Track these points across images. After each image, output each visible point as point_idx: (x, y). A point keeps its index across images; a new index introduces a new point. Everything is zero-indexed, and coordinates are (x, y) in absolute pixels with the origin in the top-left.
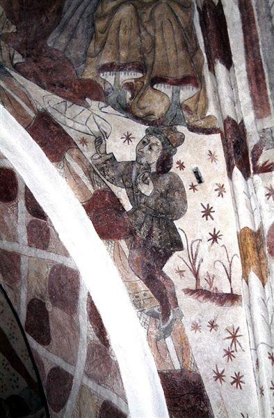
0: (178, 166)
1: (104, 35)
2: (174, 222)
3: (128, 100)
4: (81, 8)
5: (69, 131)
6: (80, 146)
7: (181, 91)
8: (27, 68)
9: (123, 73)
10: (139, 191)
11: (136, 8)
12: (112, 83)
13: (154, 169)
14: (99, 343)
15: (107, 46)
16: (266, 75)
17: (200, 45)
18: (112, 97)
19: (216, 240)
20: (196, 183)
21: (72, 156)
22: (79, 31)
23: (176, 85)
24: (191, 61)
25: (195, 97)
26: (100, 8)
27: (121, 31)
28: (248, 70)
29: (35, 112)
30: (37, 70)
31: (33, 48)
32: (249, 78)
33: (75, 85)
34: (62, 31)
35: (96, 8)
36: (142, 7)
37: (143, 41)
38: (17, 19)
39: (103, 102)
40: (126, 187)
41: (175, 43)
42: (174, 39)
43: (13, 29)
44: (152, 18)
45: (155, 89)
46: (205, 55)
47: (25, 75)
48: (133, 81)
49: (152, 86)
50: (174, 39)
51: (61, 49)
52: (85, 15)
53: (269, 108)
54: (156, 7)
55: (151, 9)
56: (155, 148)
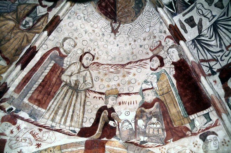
11: (15, 26)
16: (29, 82)
24: (14, 56)
27: (4, 26)
28: (26, 76)
32: (24, 78)
35: (5, 13)
36: (17, 28)
37: (7, 36)
46: (19, 59)
53: (20, 92)
54: (21, 32)
55: (19, 31)
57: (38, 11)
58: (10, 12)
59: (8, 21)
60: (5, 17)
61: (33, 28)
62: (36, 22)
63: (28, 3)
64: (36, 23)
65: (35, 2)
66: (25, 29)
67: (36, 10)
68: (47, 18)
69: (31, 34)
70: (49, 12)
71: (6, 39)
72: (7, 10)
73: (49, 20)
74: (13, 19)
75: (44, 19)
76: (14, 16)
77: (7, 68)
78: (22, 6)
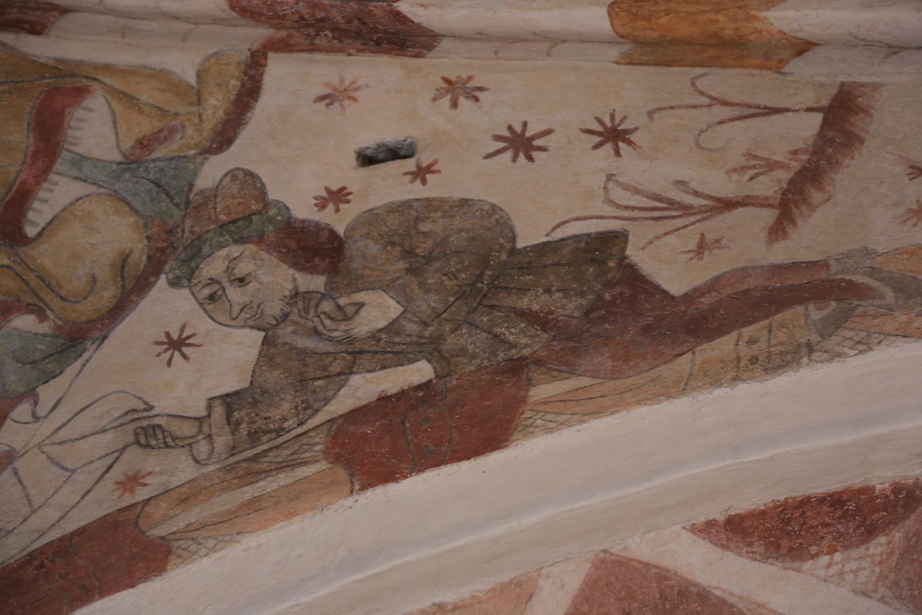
0: (331, 207)
2: (520, 244)
3: (45, 328)
5: (70, 526)
6: (141, 494)
7: (81, 150)
10: (374, 336)
13: (316, 282)
14: (897, 535)
19: (626, 132)
20: (410, 164)
21: (167, 518)
23: (52, 162)
25: (116, 105)
39: (12, 408)
40: (349, 371)
45: (40, 234)
49: (25, 241)
56: (243, 268)
77: (109, 81)
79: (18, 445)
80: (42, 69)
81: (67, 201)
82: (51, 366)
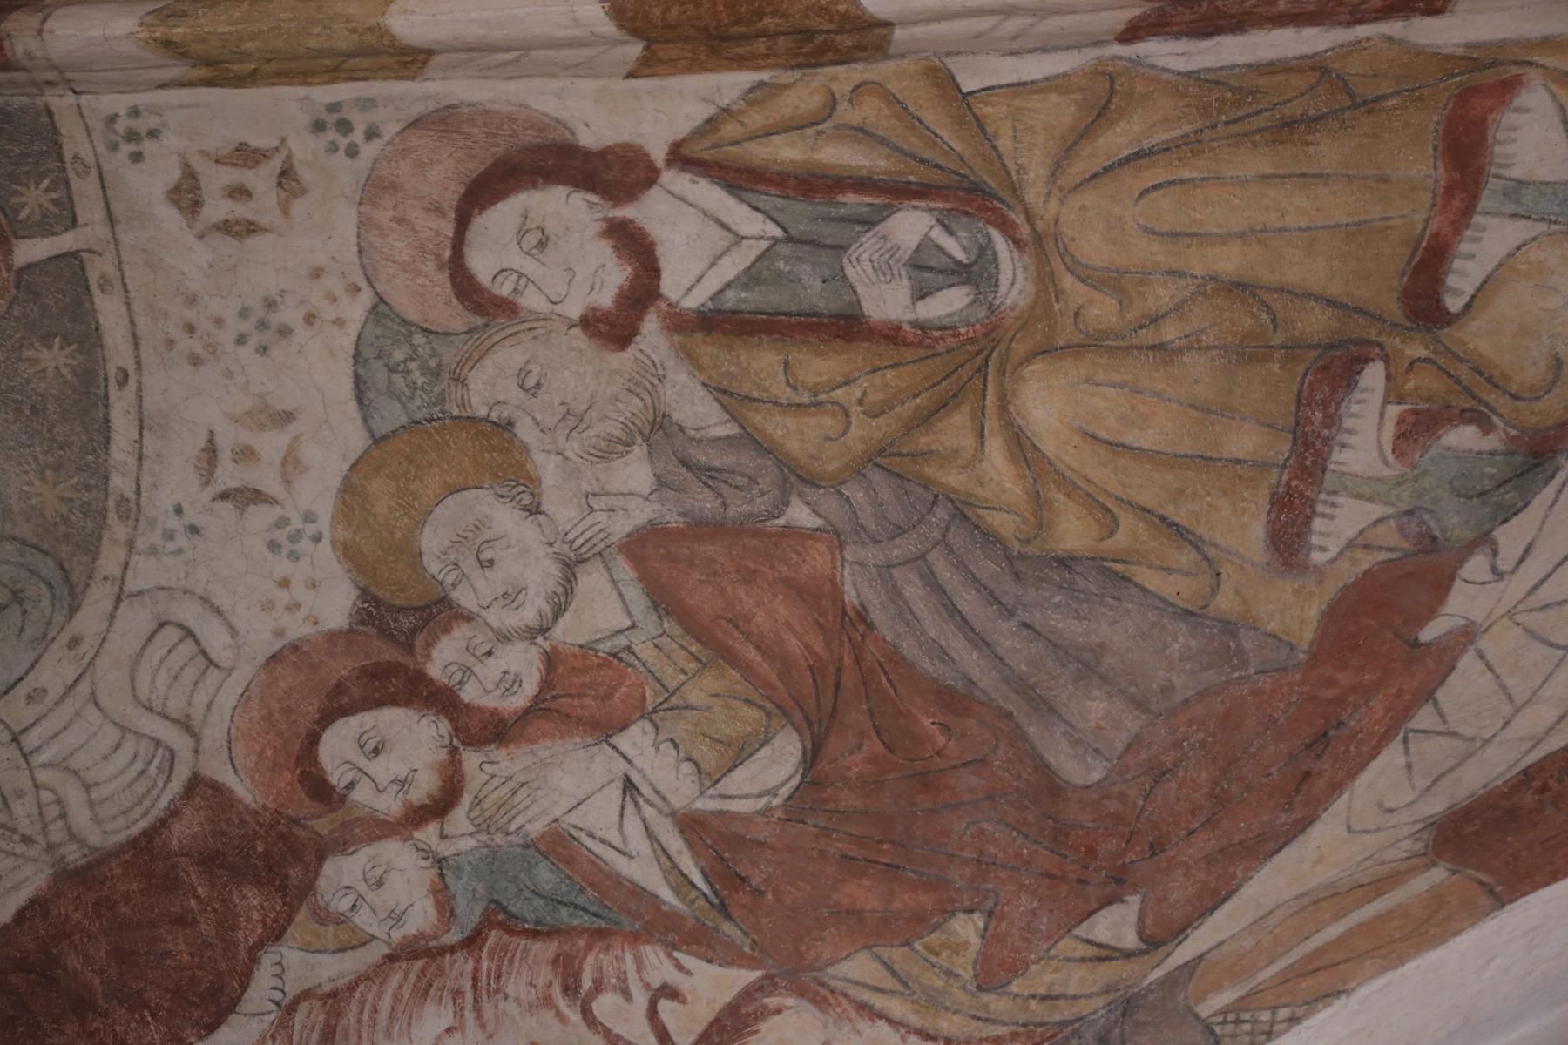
1: (1127, 521)
3: (1492, 442)
4: (967, 600)
7: (1516, 172)
8: (1180, 889)
9: (1338, 456)
12: (1378, 510)
15: (1178, 513)
17: (1306, 49)
18: (1453, 521)
22: (1072, 629)
23: (1474, 197)
24: (1371, 105)
26: (995, 520)
27: (1132, 438)
29: (1427, 867)
30: (1206, 843)
31: (1091, 852)
33: (1331, 683)
34: (1046, 709)
35: (989, 538)
38: (927, 900)
39: (1461, 562)
41: (1266, 177)
42: (1240, 182)
43: (967, 929)
44: (1114, 282)
45: (1468, 306)
47: (1211, 901)
48: (1394, 410)
49: (1448, 319)
50: (1240, 182)
51: (1133, 724)
52: (1009, 590)
54: (1065, 254)
55: (1068, 282)
57: (731, 267)
58: (938, 496)
59: (1049, 447)
60: (1039, 502)
61: (934, 176)
62: (850, 198)
63: (734, 417)
64: (862, 184)
65: (670, 364)
66: (1001, 243)
67: (731, 299)
68: (730, 130)
69: (1005, 144)
70: (659, 155)
71: (1249, 323)
72: (943, 542)
73: (731, 84)
74: (991, 424)
75: (759, 153)
76: (954, 431)
77: (1550, 62)
78: (793, 445)
79: (1477, 616)
80: (1447, 63)
81: (1500, 251)
82: (1509, 497)
